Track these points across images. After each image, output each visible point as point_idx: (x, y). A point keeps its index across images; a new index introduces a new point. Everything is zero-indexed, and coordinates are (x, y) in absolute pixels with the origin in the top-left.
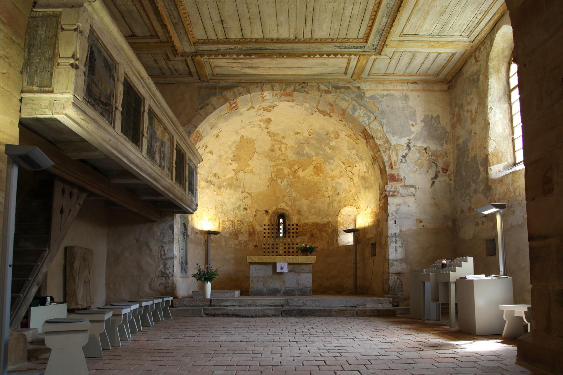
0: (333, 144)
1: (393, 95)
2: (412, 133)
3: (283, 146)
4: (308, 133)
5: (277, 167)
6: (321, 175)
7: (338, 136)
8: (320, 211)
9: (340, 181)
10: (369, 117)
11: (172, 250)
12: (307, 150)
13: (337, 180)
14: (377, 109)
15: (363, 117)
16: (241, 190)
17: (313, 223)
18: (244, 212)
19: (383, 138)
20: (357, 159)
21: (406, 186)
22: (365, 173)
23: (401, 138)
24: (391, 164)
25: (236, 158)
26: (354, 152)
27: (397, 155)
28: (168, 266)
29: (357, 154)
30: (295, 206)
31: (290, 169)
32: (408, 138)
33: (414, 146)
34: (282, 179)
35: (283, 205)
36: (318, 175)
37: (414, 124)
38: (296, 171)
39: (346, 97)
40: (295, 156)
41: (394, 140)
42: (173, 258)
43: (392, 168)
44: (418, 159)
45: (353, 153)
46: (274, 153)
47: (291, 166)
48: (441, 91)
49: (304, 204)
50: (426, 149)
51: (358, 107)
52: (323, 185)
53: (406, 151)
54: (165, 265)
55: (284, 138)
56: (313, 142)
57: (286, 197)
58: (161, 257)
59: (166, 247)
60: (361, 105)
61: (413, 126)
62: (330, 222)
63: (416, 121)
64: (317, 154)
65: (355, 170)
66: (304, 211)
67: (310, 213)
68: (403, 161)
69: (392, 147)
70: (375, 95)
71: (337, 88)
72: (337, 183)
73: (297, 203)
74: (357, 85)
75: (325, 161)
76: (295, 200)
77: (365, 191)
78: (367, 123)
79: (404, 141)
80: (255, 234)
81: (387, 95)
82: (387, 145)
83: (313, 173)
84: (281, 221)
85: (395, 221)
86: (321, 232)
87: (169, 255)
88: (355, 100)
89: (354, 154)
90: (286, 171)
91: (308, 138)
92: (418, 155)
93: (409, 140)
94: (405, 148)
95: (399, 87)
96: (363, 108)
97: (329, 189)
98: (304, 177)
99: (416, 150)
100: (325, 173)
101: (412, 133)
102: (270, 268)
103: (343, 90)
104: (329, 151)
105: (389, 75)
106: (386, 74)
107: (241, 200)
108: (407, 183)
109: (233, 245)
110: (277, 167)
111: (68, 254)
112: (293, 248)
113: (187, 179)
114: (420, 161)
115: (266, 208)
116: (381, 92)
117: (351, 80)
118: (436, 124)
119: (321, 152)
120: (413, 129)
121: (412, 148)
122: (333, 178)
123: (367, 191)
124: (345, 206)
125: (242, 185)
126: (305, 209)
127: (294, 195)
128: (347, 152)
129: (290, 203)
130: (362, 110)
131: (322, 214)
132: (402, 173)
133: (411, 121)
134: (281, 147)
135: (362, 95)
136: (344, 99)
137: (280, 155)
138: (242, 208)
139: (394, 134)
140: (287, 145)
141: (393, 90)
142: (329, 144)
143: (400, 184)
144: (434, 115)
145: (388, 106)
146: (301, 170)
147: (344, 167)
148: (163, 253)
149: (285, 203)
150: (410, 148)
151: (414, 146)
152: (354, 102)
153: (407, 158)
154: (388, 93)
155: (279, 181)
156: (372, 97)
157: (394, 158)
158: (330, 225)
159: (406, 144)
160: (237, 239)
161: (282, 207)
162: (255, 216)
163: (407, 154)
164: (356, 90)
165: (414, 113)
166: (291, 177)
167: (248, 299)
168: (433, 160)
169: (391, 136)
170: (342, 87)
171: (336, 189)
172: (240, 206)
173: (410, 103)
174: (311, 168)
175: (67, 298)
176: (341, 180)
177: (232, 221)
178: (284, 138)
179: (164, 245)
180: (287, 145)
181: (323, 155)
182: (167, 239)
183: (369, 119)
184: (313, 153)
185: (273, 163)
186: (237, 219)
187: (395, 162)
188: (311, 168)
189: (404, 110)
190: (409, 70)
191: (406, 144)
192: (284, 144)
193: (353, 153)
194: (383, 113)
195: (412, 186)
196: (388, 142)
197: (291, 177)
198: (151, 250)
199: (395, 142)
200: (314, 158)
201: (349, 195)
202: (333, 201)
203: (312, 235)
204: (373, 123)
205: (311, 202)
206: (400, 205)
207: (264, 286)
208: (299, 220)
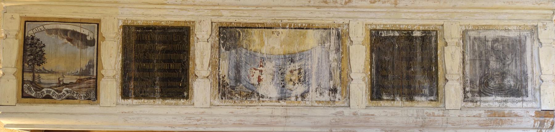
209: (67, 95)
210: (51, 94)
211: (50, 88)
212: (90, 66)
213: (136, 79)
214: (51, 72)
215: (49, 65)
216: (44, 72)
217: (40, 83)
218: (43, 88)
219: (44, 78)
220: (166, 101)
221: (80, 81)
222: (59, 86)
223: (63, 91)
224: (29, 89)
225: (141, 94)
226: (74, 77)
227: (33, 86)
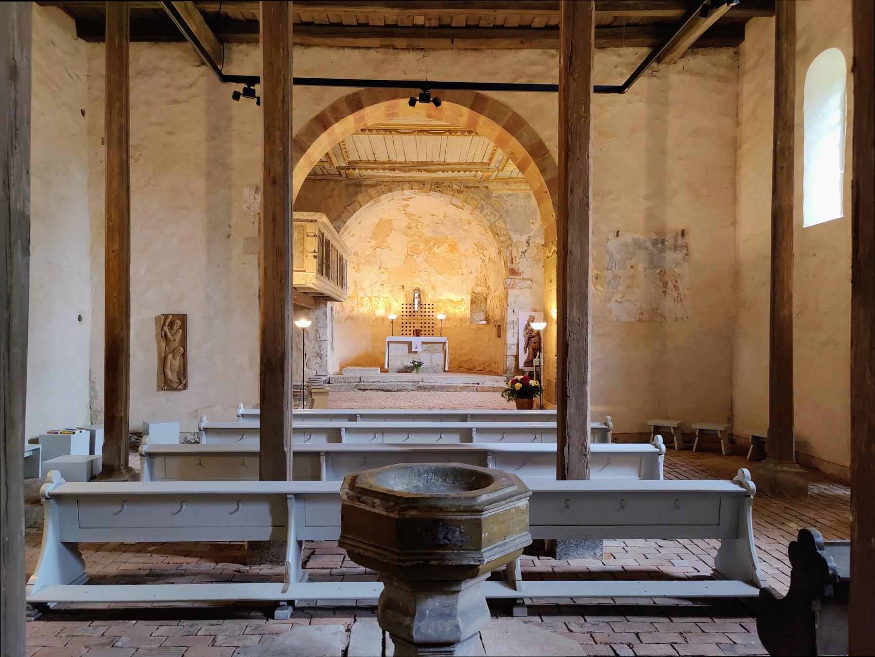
2: (532, 230)
11: (326, 334)
16: (378, 266)
25: (375, 236)
34: (419, 253)
38: (431, 248)
41: (515, 237)
51: (486, 206)
54: (320, 347)
55: (420, 217)
71: (466, 187)
79: (524, 238)
84: (416, 295)
87: (323, 338)
90: (422, 246)
97: (463, 266)
101: (532, 230)
102: (406, 347)
116: (506, 192)
120: (533, 227)
139: (516, 231)
155: (415, 256)
156: (498, 197)
157: (515, 254)
164: (484, 189)
174: (446, 245)
178: (420, 217)
182: (321, 324)
184: (448, 232)
188: (446, 245)
194: (507, 211)
196: (510, 239)
208: (434, 296)
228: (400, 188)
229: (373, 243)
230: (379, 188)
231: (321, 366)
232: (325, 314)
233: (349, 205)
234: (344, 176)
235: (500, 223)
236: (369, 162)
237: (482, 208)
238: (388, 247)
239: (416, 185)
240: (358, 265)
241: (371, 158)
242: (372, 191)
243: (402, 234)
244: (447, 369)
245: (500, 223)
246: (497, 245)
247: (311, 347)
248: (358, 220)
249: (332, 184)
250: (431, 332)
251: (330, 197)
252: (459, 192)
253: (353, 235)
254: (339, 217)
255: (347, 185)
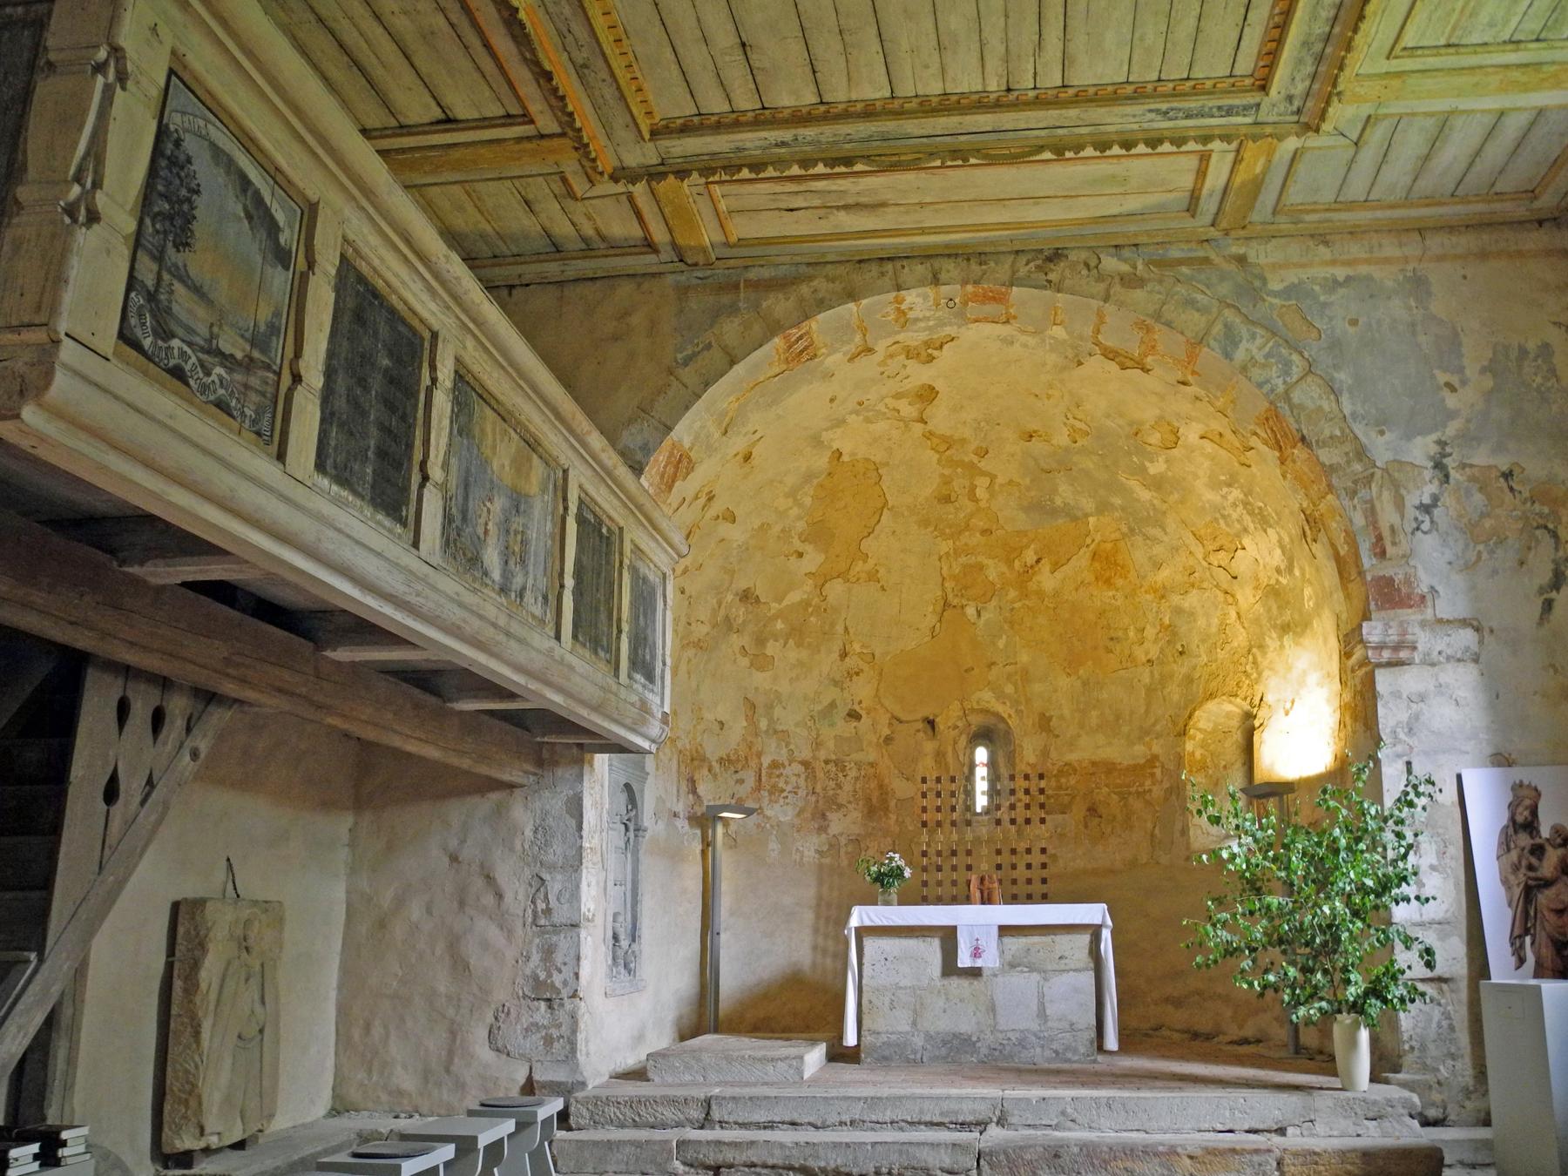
0: (1156, 468)
1: (1369, 278)
2: (1451, 415)
3: (981, 482)
4: (1065, 431)
5: (963, 560)
6: (1120, 582)
7: (1174, 439)
8: (1118, 717)
9: (1186, 605)
10: (1287, 364)
11: (575, 895)
12: (1065, 493)
13: (1175, 599)
14: (1314, 334)
15: (1264, 366)
16: (836, 647)
17: (1094, 764)
18: (845, 728)
19: (1341, 440)
20: (1247, 520)
21: (1440, 621)
22: (1278, 571)
23: (1409, 436)
24: (1380, 538)
26: (1236, 494)
27: (1400, 504)
28: (559, 958)
29: (1246, 504)
30: (1028, 701)
31: (1010, 563)
32: (1434, 437)
33: (1463, 466)
35: (987, 698)
36: (1108, 582)
37: (1455, 380)
38: (1029, 571)
39: (1199, 297)
40: (1022, 516)
41: (1382, 448)
42: (575, 926)
43: (1382, 554)
44: (1482, 515)
45: (1231, 498)
46: (950, 508)
47: (1010, 553)
48: (1549, 253)
49: (1058, 690)
50: (1507, 475)
51: (1243, 330)
52: (1126, 620)
53: (1432, 488)
54: (548, 952)
55: (983, 453)
56: (1088, 463)
57: (995, 670)
58: (534, 923)
59: (555, 884)
60: (1253, 323)
61: (1453, 389)
62: (1155, 758)
63: (1461, 370)
64: (1103, 508)
65: (1242, 563)
66: (1062, 717)
67: (1082, 726)
68: (1426, 526)
69: (1378, 473)
70: (1301, 282)
71: (1163, 263)
72: (1178, 611)
73: (1037, 687)
74: (1237, 249)
75: (1132, 530)
76: (1026, 676)
77: (1281, 638)
78: (1281, 388)
79: (1420, 450)
80: (886, 810)
81: (1348, 279)
82: (1358, 467)
83: (1090, 577)
85: (1409, 764)
86: (1123, 797)
87: (561, 914)
88: (1229, 306)
89: (1235, 505)
91: (1067, 449)
92: (1478, 498)
93: (1441, 443)
94: (1428, 474)
95: (1390, 249)
96: (1259, 331)
97: (1150, 632)
98: (1057, 593)
99: (1472, 479)
100: (1132, 575)
101: (1451, 415)
103: (1185, 269)
104: (1145, 495)
105: (1351, 205)
106: (1339, 205)
107: (836, 683)
108: (1444, 609)
109: (810, 854)
110: (963, 560)
111: (181, 930)
112: (1029, 866)
113: (625, 627)
114: (1488, 523)
115: (927, 712)
117: (1213, 233)
118: (1539, 380)
119: (1117, 501)
120: (1451, 401)
121: (1452, 473)
122: (1162, 593)
123: (1287, 640)
124: (1211, 696)
125: (840, 628)
126: (1066, 712)
127: (1024, 658)
128: (1210, 496)
129: (1009, 689)
130: (1259, 341)
131: (1126, 729)
132: (1421, 573)
133: (1445, 370)
134: (973, 488)
135: (1257, 283)
136: (1190, 303)
137: (972, 515)
138: (842, 711)
140: (993, 477)
141: (1368, 261)
142: (1145, 469)
143: (1420, 617)
144: (1531, 345)
145: (1354, 322)
146: (1045, 566)
147: (1199, 552)
148: (541, 906)
149: (992, 690)
150: (1447, 476)
151: (1463, 466)
152: (1227, 312)
153: (1436, 512)
154: (1350, 271)
155: (971, 611)
156: (1289, 292)
157: (1388, 515)
158: (1158, 771)
159: (1432, 458)
160: (822, 829)
161: (984, 705)
162: (888, 740)
163: (1435, 499)
164: (1232, 267)
165: (1452, 343)
166: (1012, 594)
167: (855, 1082)
168: (1541, 515)
169: (1373, 435)
170: (1180, 262)
171: (1175, 634)
172: (833, 705)
173: (1436, 307)
174: (1082, 560)
175: (167, 1108)
176: (1192, 600)
177: (806, 764)
179: (546, 876)
180: (993, 477)
181: (1123, 509)
183: (1286, 372)
184: (1088, 504)
185: (945, 546)
186: (822, 755)
187: (1392, 529)
188: (1082, 560)
189: (1414, 334)
190: (1425, 185)
191: (1432, 458)
192: (984, 474)
193: (1231, 498)
194: (1336, 345)
195: (1464, 623)
196: (1361, 453)
197: (1012, 594)
198: (500, 896)
199: (1389, 456)
200: (1091, 520)
201: (1221, 655)
202: (1165, 679)
203: (1092, 810)
204: (1303, 385)
205: (1085, 684)
206: (1422, 698)
207: (914, 1024)
208: (1045, 753)
209: (221, 392)
210: (187, 368)
211: (190, 344)
212: (273, 329)
213: (341, 425)
214: (197, 290)
215: (198, 262)
216: (184, 278)
217: (169, 311)
218: (174, 336)
219: (182, 301)
220: (380, 517)
221: (249, 365)
222: (208, 352)
223: (214, 377)
224: (141, 315)
225: (343, 478)
226: (241, 341)
227: (154, 316)
228: (887, 281)
229: (813, 560)
230: (805, 289)
231: (549, 1041)
232: (575, 808)
233: (687, 362)
234: (667, 254)
235: (1309, 394)
236: (733, 123)
237: (1230, 340)
238: (873, 576)
239: (949, 268)
240: (760, 641)
241: (746, 101)
242: (780, 305)
243: (925, 523)
244: (1112, 1042)
245: (1309, 394)
246: (1298, 501)
247: (510, 954)
248: (738, 443)
249: (625, 289)
250: (1037, 888)
251: (616, 338)
252: (1132, 281)
253: (731, 517)
254: (644, 409)
255: (683, 291)
